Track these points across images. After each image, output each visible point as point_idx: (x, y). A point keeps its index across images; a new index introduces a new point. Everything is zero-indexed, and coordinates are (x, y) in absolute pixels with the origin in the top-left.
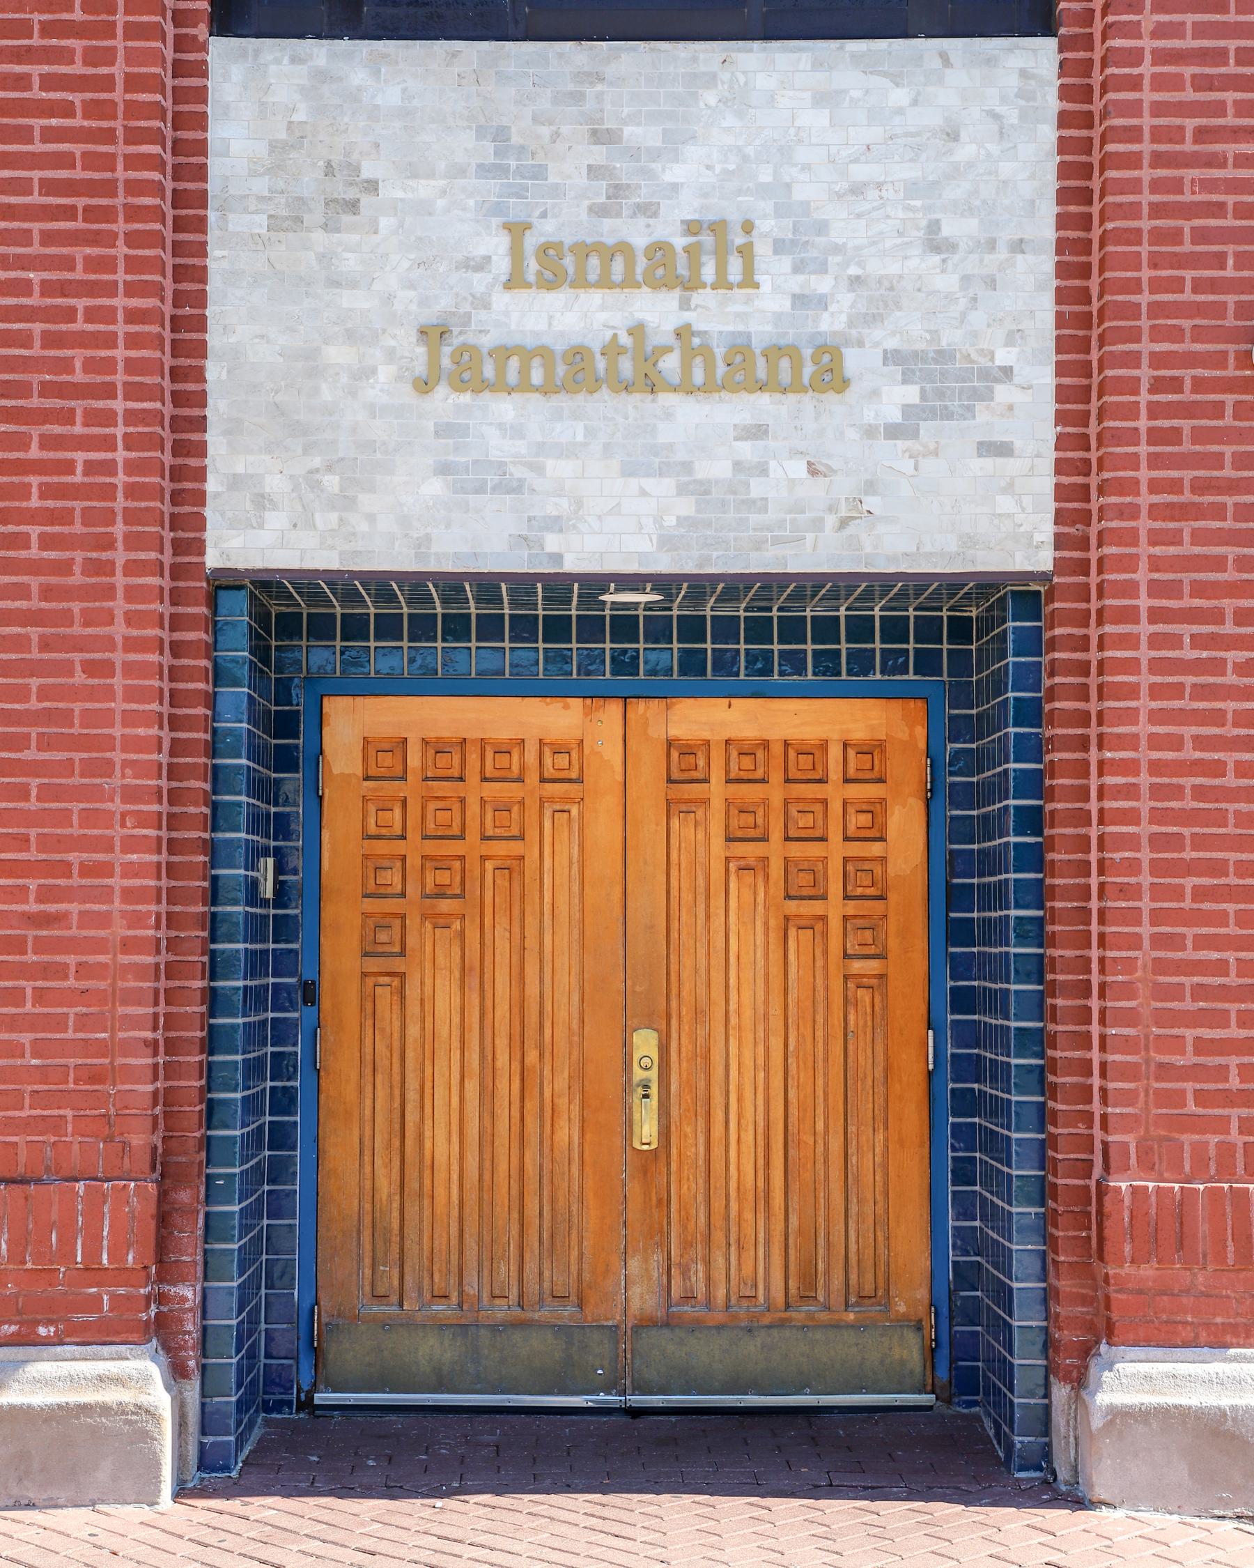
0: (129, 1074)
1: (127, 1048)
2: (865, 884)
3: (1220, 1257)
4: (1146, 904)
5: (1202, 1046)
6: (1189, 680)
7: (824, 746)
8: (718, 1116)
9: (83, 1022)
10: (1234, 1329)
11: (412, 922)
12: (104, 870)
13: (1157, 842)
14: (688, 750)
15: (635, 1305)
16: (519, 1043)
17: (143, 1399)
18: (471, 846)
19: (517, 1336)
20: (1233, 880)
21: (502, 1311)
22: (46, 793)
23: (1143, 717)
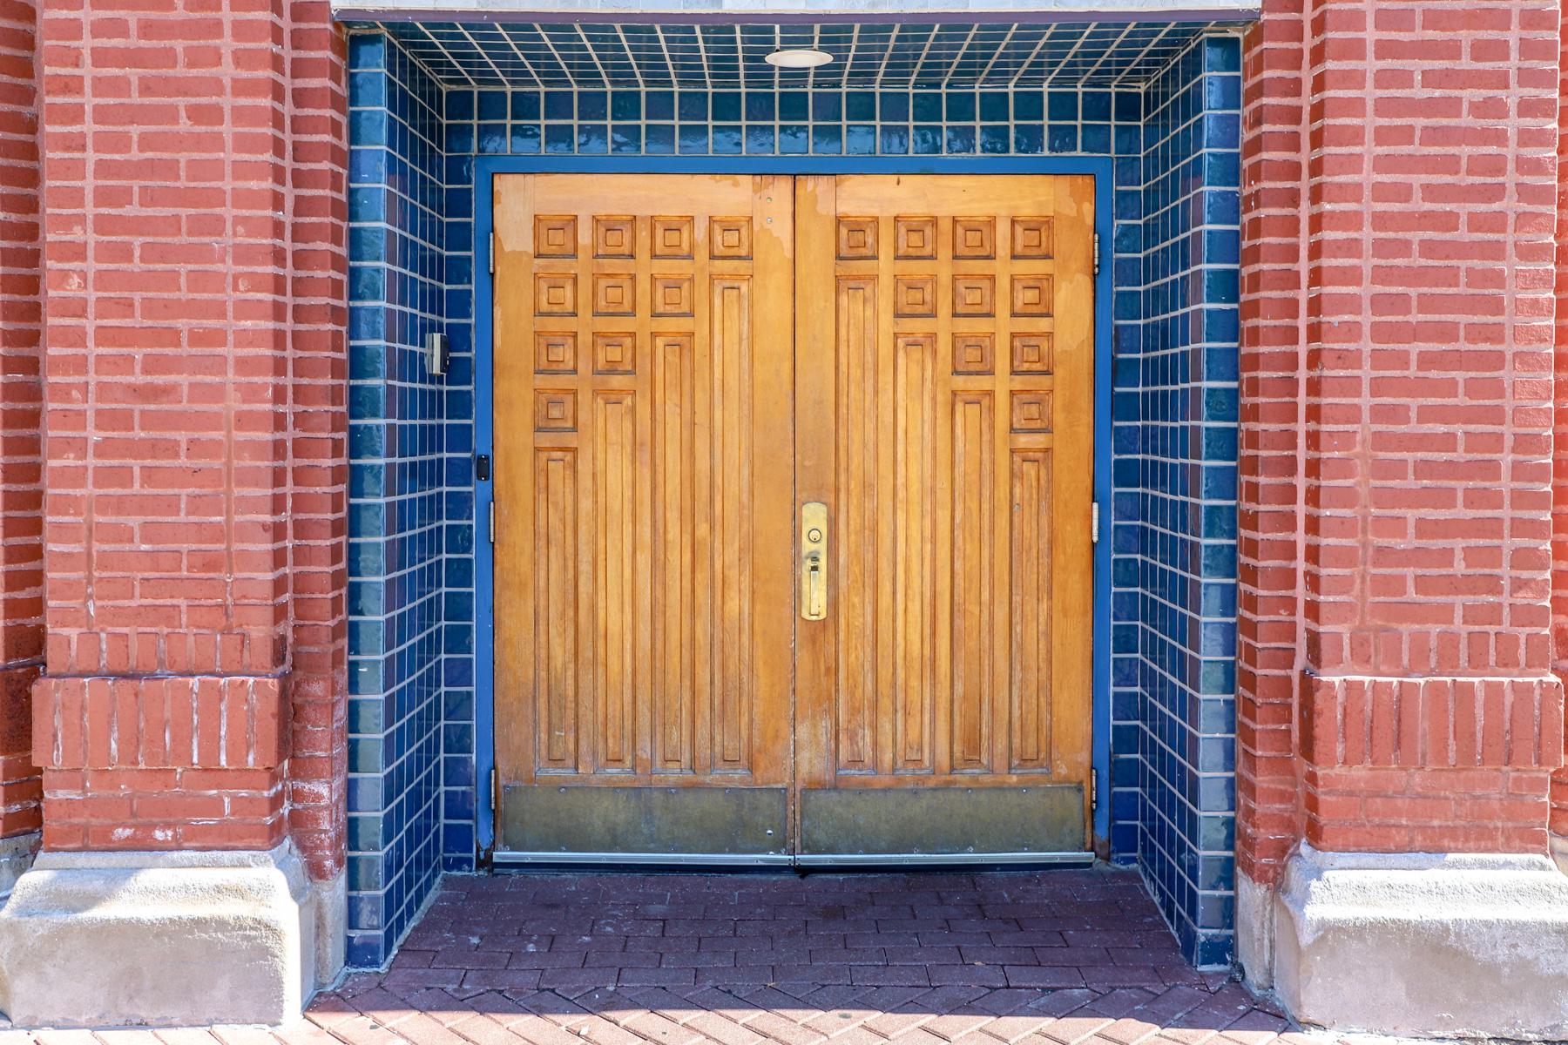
0: (246, 559)
1: (243, 533)
2: (1032, 359)
3: (1441, 756)
4: (1366, 373)
5: (1423, 528)
6: (1420, 122)
7: (992, 222)
8: (886, 587)
9: (196, 504)
10: (1452, 832)
11: (584, 398)
12: (217, 337)
13: (1378, 303)
14: (857, 227)
15: (804, 769)
16: (689, 517)
17: (263, 914)
18: (641, 323)
19: (689, 799)
20: (1462, 345)
21: (674, 774)
22: (150, 253)
23: (1367, 164)
